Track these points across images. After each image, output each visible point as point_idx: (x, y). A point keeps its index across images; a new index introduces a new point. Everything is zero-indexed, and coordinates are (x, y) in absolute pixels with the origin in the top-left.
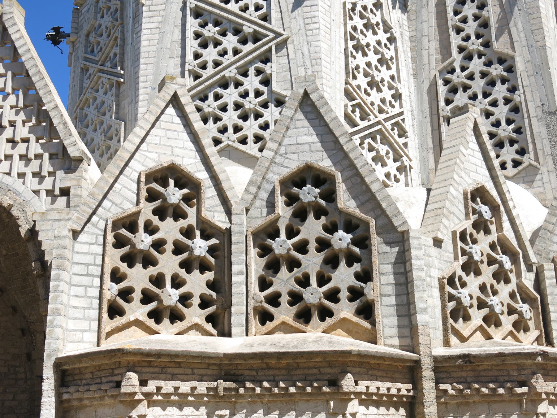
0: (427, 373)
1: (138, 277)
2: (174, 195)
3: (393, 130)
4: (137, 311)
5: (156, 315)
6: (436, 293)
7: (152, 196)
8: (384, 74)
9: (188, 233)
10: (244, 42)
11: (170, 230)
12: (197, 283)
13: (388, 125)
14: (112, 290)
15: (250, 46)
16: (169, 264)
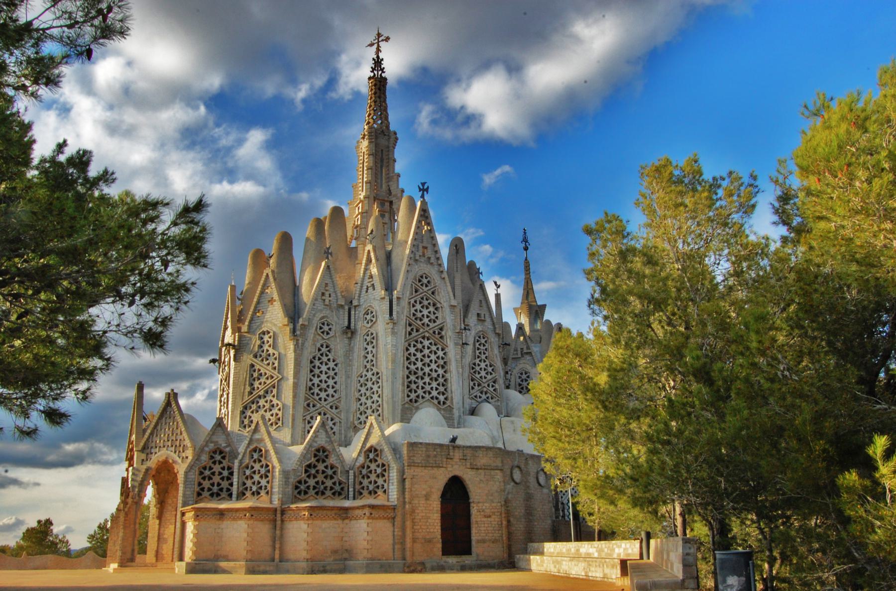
0: (279, 512)
1: (206, 484)
2: (218, 457)
3: (331, 407)
4: (206, 494)
5: (212, 495)
6: (290, 487)
7: (212, 457)
8: (331, 382)
9: (223, 469)
10: (267, 378)
11: (217, 468)
12: (225, 484)
13: (328, 407)
14: (197, 489)
15: (270, 381)
16: (216, 479)
